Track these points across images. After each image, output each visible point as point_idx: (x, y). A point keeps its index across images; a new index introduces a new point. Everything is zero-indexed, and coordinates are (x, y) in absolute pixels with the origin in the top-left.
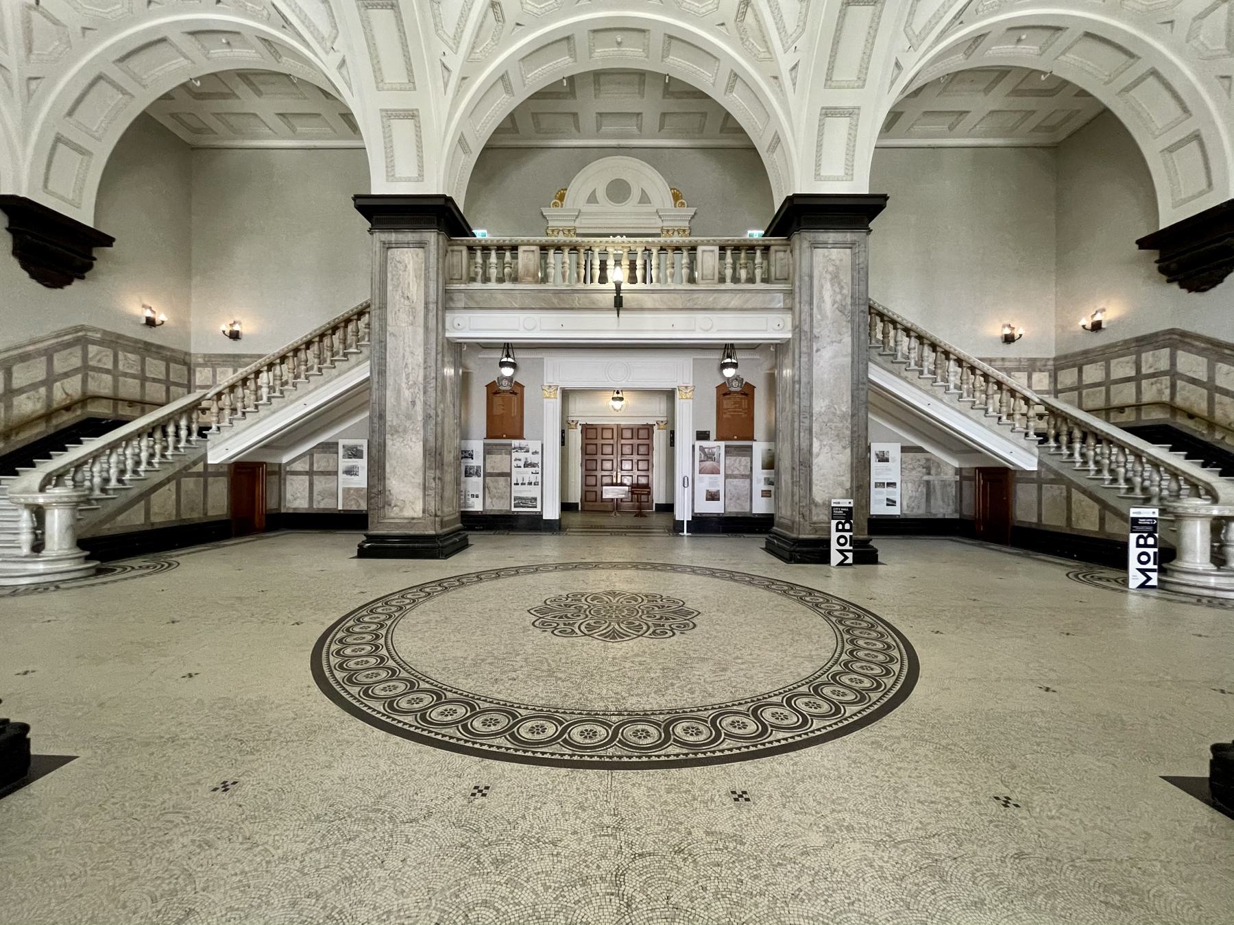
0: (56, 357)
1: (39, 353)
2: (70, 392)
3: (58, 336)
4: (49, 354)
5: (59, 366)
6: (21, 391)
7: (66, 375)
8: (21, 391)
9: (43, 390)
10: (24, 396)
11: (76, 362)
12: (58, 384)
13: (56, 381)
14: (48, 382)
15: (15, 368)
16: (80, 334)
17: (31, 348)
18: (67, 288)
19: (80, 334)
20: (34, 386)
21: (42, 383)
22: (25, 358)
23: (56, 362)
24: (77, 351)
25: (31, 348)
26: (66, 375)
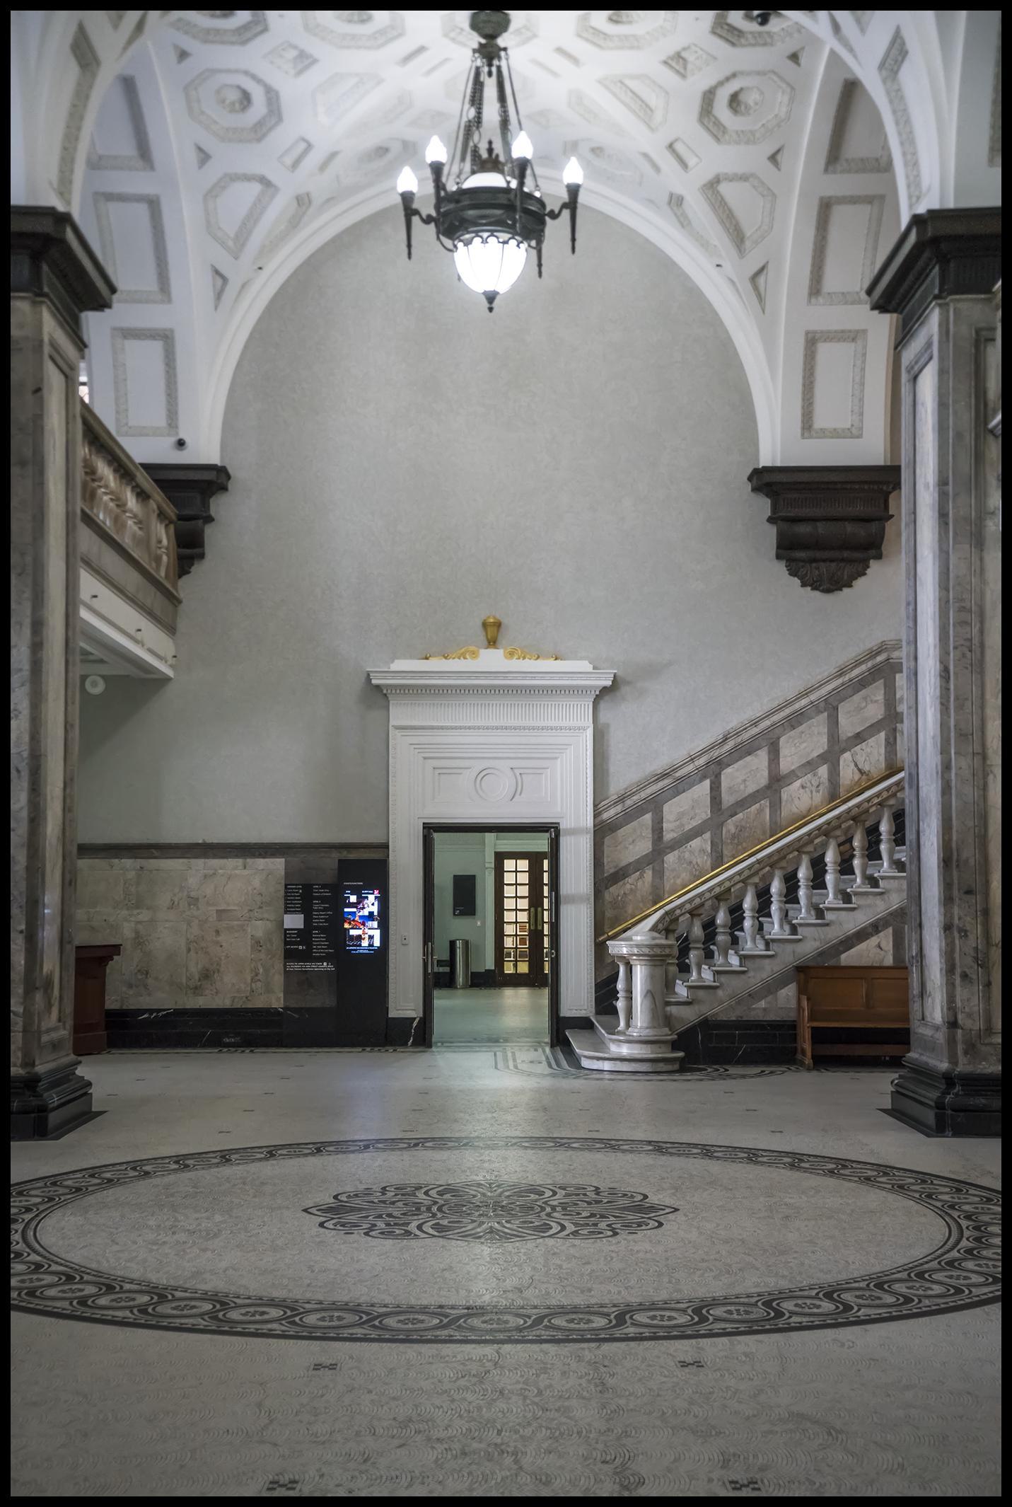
0: (843, 709)
1: (816, 708)
2: (866, 768)
3: (841, 673)
4: (830, 707)
5: (849, 724)
6: (793, 775)
7: (859, 738)
8: (793, 775)
9: (823, 771)
10: (797, 784)
11: (875, 711)
12: (847, 755)
13: (843, 751)
14: (830, 758)
15: (782, 740)
16: (879, 659)
17: (804, 702)
18: (860, 583)
19: (879, 659)
20: (810, 766)
21: (823, 758)
22: (795, 720)
23: (842, 719)
24: (877, 692)
25: (804, 702)
26: (859, 738)
